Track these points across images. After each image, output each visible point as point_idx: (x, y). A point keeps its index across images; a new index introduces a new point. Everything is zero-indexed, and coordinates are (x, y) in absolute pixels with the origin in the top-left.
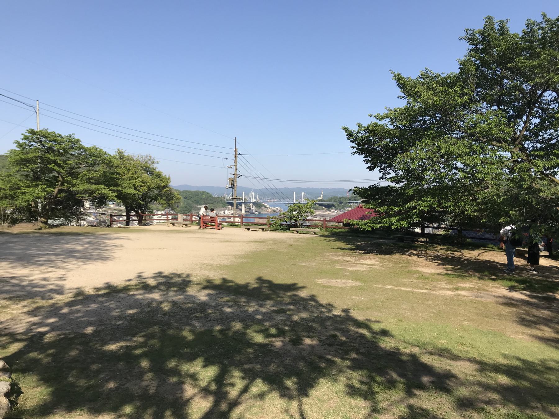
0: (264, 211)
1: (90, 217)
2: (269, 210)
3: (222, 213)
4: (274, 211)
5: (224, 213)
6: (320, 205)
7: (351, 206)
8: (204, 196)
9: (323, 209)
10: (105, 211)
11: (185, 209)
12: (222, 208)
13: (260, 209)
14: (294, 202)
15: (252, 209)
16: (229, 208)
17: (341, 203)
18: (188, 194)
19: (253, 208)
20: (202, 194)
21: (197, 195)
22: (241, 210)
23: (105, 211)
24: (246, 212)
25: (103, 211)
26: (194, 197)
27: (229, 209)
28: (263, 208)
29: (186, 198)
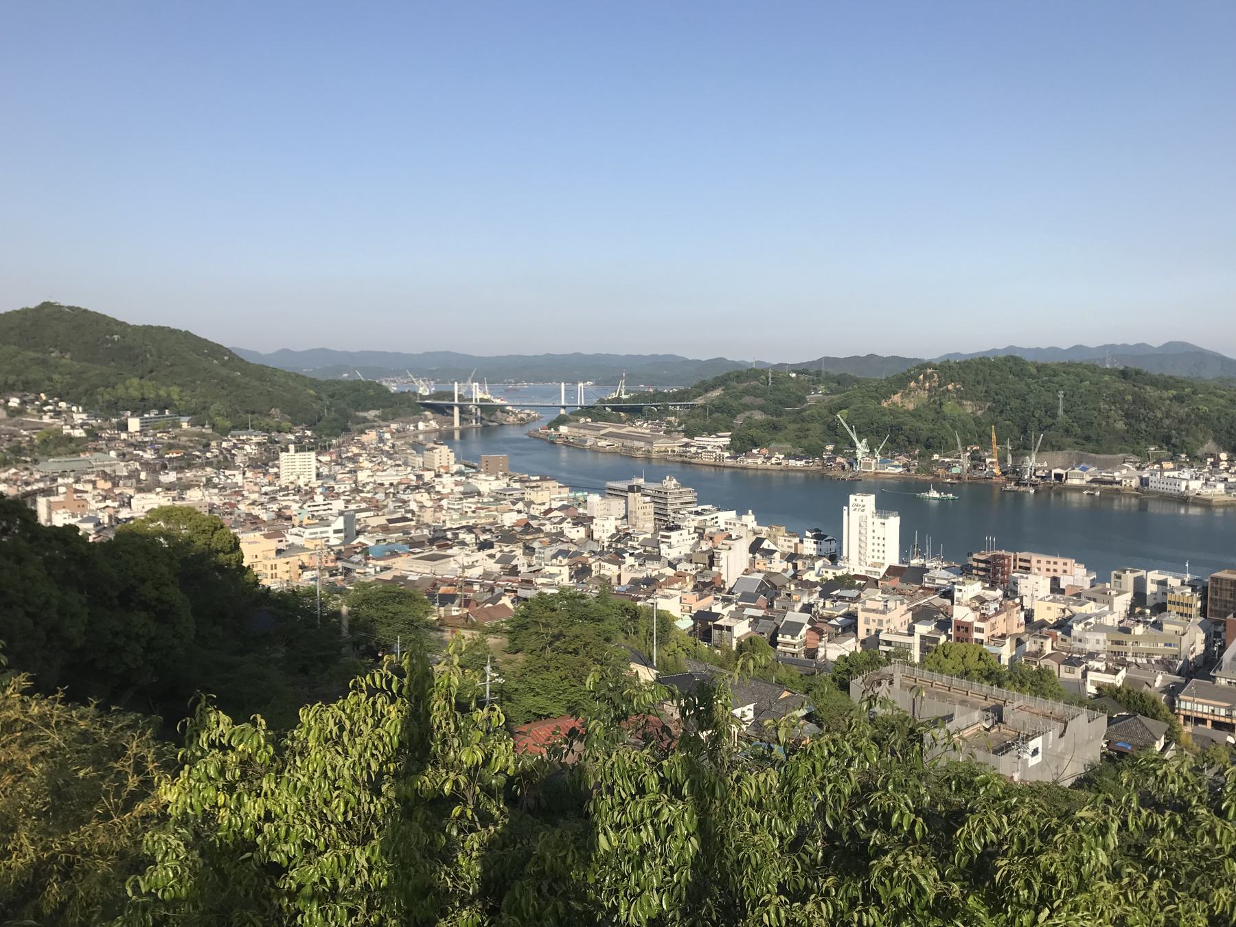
3: (412, 428)
4: (522, 419)
5: (416, 427)
6: (614, 409)
7: (674, 414)
8: (371, 392)
10: (174, 438)
11: (335, 424)
14: (563, 404)
16: (426, 416)
18: (338, 387)
21: (358, 390)
23: (174, 438)
25: (169, 438)
27: (426, 420)
28: (499, 413)
29: (332, 396)
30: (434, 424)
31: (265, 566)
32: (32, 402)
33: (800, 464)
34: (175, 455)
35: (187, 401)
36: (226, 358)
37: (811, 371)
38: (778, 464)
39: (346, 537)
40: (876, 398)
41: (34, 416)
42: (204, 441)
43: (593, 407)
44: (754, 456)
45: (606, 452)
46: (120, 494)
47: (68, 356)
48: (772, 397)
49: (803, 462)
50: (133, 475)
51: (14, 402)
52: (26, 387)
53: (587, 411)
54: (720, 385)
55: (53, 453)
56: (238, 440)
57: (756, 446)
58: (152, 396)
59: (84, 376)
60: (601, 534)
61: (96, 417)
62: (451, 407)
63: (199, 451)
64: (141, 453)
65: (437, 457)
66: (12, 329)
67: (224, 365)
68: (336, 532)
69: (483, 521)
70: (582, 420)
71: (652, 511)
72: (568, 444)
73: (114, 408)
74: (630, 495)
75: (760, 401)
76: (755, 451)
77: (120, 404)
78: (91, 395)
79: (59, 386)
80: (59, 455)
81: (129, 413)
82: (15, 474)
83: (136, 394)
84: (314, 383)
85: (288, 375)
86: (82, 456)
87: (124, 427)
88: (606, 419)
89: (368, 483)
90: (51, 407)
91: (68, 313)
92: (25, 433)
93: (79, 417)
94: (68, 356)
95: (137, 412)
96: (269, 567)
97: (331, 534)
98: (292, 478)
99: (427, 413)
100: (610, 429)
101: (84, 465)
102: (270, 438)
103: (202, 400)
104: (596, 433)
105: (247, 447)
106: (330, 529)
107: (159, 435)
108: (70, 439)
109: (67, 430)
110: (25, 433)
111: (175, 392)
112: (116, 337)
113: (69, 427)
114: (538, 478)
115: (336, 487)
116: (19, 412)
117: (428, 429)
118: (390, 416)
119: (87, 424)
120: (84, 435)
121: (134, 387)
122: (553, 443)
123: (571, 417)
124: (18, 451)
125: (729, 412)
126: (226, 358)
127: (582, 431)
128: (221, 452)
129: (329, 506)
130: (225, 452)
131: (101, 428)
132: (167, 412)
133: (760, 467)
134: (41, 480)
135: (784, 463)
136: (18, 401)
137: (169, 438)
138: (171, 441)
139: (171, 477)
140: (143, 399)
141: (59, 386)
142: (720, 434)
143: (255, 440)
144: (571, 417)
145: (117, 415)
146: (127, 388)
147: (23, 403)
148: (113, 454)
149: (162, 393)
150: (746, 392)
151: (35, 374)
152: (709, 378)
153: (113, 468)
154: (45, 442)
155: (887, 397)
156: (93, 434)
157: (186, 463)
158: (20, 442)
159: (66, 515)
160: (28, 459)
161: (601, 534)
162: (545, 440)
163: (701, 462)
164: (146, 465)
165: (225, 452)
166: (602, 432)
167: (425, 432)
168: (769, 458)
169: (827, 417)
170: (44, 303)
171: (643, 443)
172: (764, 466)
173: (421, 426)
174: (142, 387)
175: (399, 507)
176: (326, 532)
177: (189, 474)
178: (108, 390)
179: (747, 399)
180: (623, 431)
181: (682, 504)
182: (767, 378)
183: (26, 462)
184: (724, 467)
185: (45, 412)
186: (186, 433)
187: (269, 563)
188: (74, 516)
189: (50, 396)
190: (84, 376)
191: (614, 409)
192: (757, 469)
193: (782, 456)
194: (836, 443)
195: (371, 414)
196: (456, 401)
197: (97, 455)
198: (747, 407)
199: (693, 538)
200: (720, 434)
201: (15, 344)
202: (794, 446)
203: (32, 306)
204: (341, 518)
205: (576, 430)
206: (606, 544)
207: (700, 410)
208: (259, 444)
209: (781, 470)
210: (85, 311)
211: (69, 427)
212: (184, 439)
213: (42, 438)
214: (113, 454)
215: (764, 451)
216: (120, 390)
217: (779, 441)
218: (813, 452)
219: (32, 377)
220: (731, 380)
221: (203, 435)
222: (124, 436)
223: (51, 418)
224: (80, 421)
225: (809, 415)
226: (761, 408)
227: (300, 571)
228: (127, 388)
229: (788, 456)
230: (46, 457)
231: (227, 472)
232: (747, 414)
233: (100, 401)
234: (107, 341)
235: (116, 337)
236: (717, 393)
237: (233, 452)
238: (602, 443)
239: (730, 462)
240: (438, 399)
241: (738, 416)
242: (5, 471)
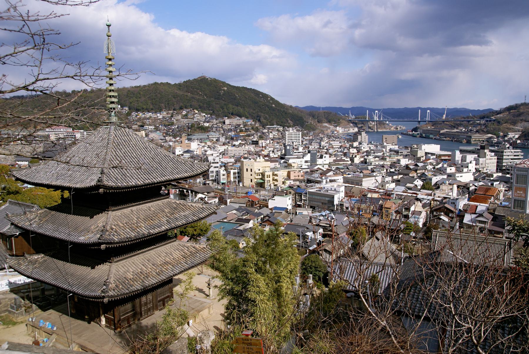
14: (419, 120)
27: (352, 127)
39: (311, 165)
68: (306, 162)
71: (496, 161)
89: (326, 146)
97: (303, 163)
115: (310, 147)
117: (354, 131)
166: (441, 132)
176: (301, 162)
204: (309, 154)
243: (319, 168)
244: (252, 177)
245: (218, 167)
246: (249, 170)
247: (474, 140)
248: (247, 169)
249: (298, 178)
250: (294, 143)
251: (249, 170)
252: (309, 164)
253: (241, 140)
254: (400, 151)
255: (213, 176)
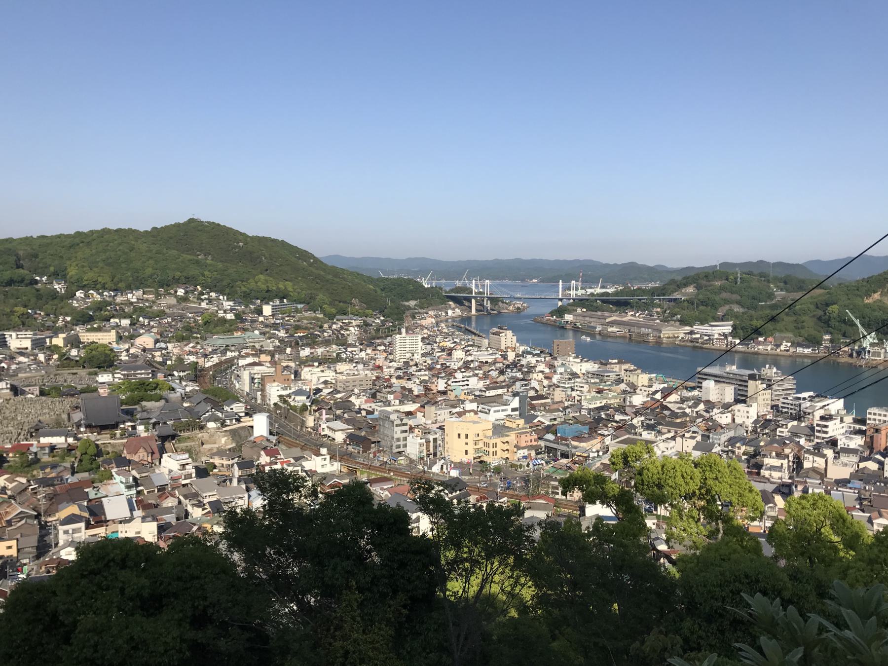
0: (503, 309)
1: (279, 331)
2: (511, 308)
3: (444, 314)
4: (519, 308)
5: (447, 313)
6: (603, 301)
7: (659, 306)
9: (611, 311)
12: (440, 306)
13: (497, 307)
14: (560, 297)
15: (485, 304)
16: (450, 305)
17: (640, 300)
18: (386, 283)
19: (488, 304)
20: (408, 284)
21: (401, 285)
22: (470, 307)
23: (298, 321)
24: (477, 310)
25: (294, 321)
26: (395, 288)
27: (453, 309)
28: (500, 304)
30: (458, 312)
31: (487, 445)
32: (192, 292)
33: (808, 351)
34: (302, 334)
35: (299, 293)
36: (312, 261)
37: (756, 272)
38: (788, 351)
40: (861, 296)
41: (195, 303)
42: (320, 323)
43: (587, 300)
44: (759, 343)
45: (616, 337)
46: (287, 366)
47: (210, 258)
48: (747, 293)
49: (810, 350)
50: (280, 350)
51: (181, 292)
52: (188, 281)
53: (581, 302)
54: (691, 284)
55: (214, 331)
56: (343, 323)
57: (761, 335)
58: (274, 288)
59: (226, 273)
60: (745, 420)
61: (240, 304)
62: (469, 300)
63: (319, 332)
64: (277, 332)
65: (503, 339)
66: (171, 238)
67: (311, 265)
68: (513, 410)
69: (612, 401)
70: (579, 310)
72: (576, 330)
73: (247, 298)
74: (751, 383)
75: (735, 297)
76: (761, 339)
77: (253, 294)
78: (232, 287)
79: (209, 280)
80: (217, 333)
81: (259, 301)
82: (193, 347)
83: (264, 287)
84: (370, 280)
85: (351, 273)
86: (236, 335)
87: (260, 312)
88: (597, 309)
90: (206, 296)
91: (207, 226)
92: (190, 315)
93: (228, 305)
94: (210, 258)
95: (266, 300)
96: (491, 446)
98: (408, 355)
99: (451, 303)
100: (614, 318)
101: (241, 341)
102: (364, 321)
103: (309, 292)
104: (603, 321)
105: (351, 329)
106: (509, 408)
107: (287, 319)
108: (224, 321)
109: (221, 314)
110: (190, 315)
111: (289, 286)
112: (241, 244)
113: (222, 312)
114: (616, 361)
116: (185, 299)
118: (425, 305)
119: (234, 309)
120: (233, 317)
121: (262, 281)
122: (562, 328)
123: (569, 307)
124: (188, 329)
125: (713, 305)
126: (312, 261)
127: (587, 319)
128: (333, 333)
129: (466, 383)
130: (336, 332)
131: (244, 313)
132: (285, 301)
133: (771, 352)
134: (214, 352)
135: (792, 350)
136: (183, 291)
137: (294, 321)
138: (297, 323)
139: (305, 352)
140: (268, 291)
141: (209, 280)
142: (712, 324)
143: (354, 323)
144: (569, 307)
145: (254, 304)
146: (256, 283)
147: (186, 292)
148: (257, 332)
149: (281, 286)
150: (722, 289)
151: (194, 271)
152: (679, 278)
153: (261, 344)
154: (206, 323)
155: (868, 295)
156: (239, 317)
157: (312, 341)
158: (188, 322)
159: (279, 388)
160: (199, 336)
161: (745, 420)
162: (555, 326)
163: (713, 347)
164: (281, 341)
165: (336, 332)
166: (608, 320)
167: (453, 318)
168: (778, 346)
169: (814, 311)
170: (190, 219)
171: (650, 330)
172: (774, 352)
173: (450, 312)
174: (267, 281)
175: (526, 385)
177: (320, 351)
178: (244, 283)
179: (725, 295)
180: (625, 319)
181: (783, 390)
182: (736, 279)
183: (197, 338)
184: (736, 352)
185: (203, 300)
186: (306, 318)
187: (492, 442)
188: (285, 389)
189: (204, 287)
190: (226, 273)
191: (603, 301)
192: (768, 355)
193: (789, 344)
194: (831, 333)
195: (412, 303)
196: (474, 295)
197: (248, 334)
198: (727, 302)
199: (843, 427)
200: (712, 324)
201: (174, 249)
202: (796, 336)
203: (182, 222)
204: (517, 398)
205: (582, 318)
206: (750, 429)
207: (686, 304)
208: (358, 326)
209: (790, 356)
210: (219, 225)
211: (222, 312)
212: (305, 321)
213: (205, 320)
214: (257, 332)
215: (770, 339)
216: (252, 284)
217: (781, 331)
218: (814, 342)
219: (191, 273)
220: (702, 279)
221: (317, 319)
222: (261, 319)
223: (207, 304)
224: (229, 307)
225: (800, 309)
226: (739, 303)
227: (515, 450)
228: (256, 283)
229: (795, 344)
230: (209, 335)
231: (349, 349)
232: (727, 307)
233: (239, 292)
234: (235, 247)
235: (241, 244)
236: (691, 290)
237: (342, 332)
238: (610, 329)
239: (740, 348)
240: (457, 293)
241: (720, 309)
242: (186, 345)
243: (539, 421)
244: (466, 447)
245: (406, 431)
246: (463, 436)
247: (666, 336)
248: (459, 435)
249: (531, 444)
250: (415, 355)
251: (463, 436)
252: (517, 413)
253: (308, 345)
254: (606, 374)
255: (398, 447)
